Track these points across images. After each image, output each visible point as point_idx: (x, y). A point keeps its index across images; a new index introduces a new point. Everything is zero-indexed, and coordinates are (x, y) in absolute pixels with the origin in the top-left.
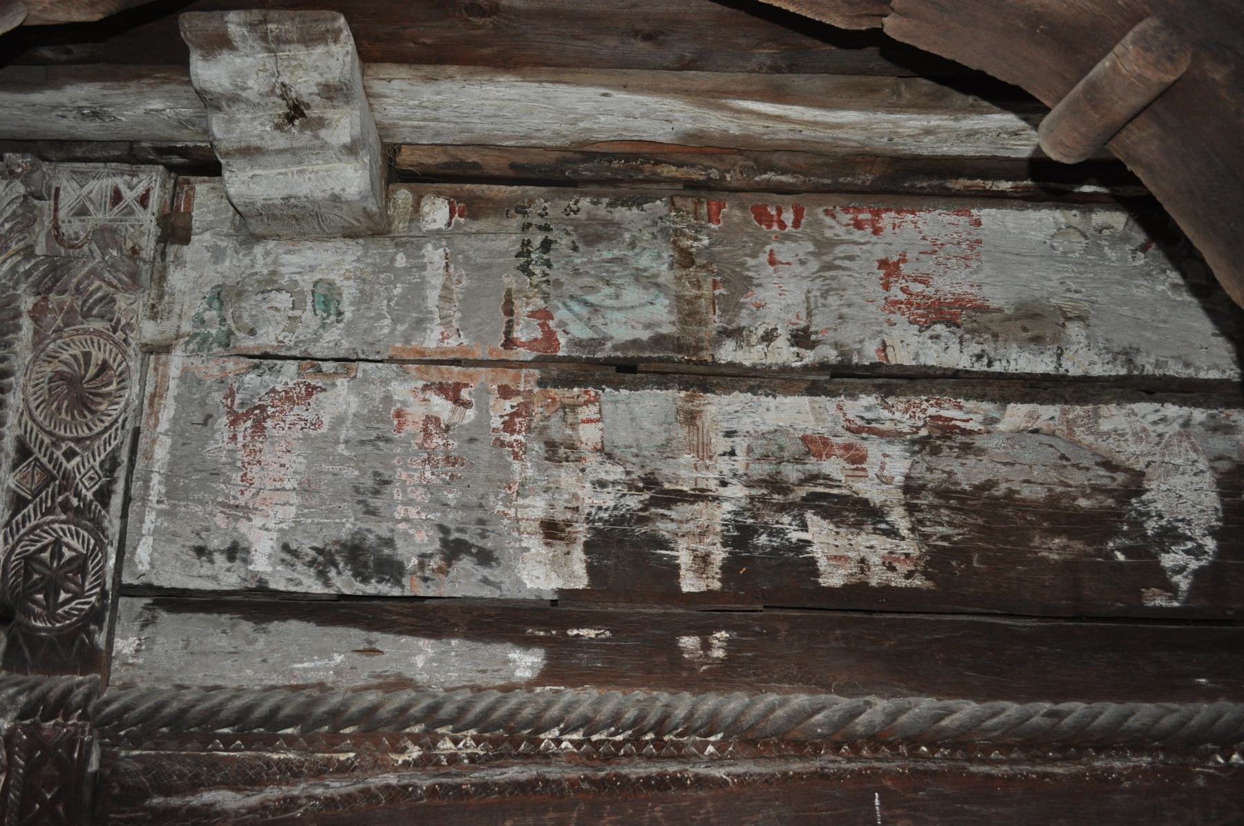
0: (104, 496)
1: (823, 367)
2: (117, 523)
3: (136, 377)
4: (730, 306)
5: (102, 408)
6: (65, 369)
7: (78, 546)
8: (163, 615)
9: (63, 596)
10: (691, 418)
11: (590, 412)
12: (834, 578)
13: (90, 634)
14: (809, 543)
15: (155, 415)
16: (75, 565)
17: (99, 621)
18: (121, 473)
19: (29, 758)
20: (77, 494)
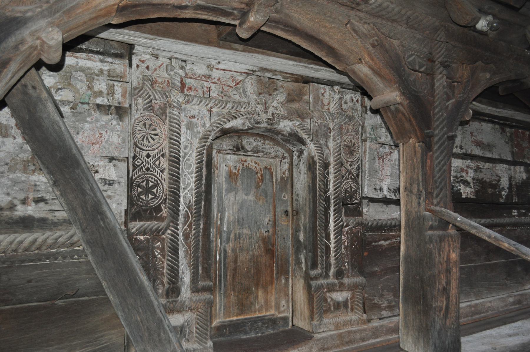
0: (358, 175)
1: (463, 154)
8: (371, 203)
9: (353, 199)
12: (464, 196)
14: (460, 189)
15: (365, 156)
18: (360, 170)
19: (351, 236)
20: (353, 175)
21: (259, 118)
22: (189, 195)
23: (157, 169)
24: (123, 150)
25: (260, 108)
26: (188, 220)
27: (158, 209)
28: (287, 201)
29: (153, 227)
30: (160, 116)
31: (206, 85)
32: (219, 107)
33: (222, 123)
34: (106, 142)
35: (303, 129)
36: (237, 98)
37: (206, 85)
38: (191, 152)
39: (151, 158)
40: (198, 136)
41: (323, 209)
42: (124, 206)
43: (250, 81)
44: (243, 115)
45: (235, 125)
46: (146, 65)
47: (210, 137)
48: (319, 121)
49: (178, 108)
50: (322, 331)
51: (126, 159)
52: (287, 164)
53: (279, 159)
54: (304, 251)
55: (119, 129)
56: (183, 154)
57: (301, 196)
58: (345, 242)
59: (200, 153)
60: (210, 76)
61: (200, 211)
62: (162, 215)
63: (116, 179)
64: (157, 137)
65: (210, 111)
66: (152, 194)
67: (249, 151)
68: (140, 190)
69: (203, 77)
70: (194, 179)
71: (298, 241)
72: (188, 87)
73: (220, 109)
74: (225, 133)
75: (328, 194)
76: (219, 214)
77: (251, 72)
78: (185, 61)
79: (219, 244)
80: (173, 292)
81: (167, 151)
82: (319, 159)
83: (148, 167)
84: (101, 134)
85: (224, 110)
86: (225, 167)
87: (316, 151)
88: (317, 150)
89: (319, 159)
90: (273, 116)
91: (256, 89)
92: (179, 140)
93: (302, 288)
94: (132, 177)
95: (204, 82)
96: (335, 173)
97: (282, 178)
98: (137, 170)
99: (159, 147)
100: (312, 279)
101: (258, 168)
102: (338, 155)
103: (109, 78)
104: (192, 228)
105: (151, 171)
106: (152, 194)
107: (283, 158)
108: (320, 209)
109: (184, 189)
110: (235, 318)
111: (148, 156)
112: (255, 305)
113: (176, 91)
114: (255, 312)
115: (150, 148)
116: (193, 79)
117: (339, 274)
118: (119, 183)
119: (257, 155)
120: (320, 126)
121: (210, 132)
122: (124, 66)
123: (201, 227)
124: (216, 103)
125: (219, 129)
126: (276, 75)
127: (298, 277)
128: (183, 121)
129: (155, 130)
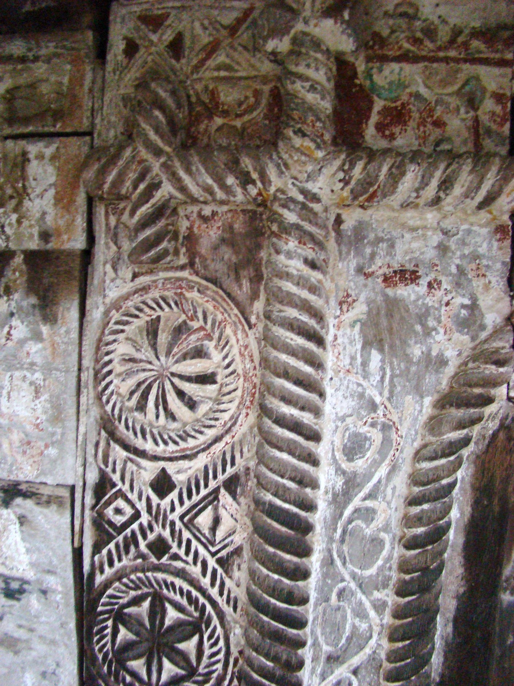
24: (52, 451)
30: (229, 283)
31: (492, 86)
37: (492, 86)
38: (382, 471)
39: (174, 495)
40: (429, 379)
46: (169, 36)
49: (305, 237)
51: (66, 494)
55: (38, 360)
56: (340, 483)
63: (30, 575)
64: (211, 389)
66: (179, 658)
68: (124, 634)
72: (385, 111)
83: (160, 539)
94: (92, 576)
95: (482, 70)
98: (112, 546)
99: (217, 439)
103: (7, 131)
105: (176, 557)
106: (179, 658)
109: (333, 660)
111: (163, 485)
113: (297, 141)
115: (172, 447)
116: (415, 59)
118: (44, 592)
121: (499, 363)
122: (76, 61)
128: (345, 302)
129: (199, 353)
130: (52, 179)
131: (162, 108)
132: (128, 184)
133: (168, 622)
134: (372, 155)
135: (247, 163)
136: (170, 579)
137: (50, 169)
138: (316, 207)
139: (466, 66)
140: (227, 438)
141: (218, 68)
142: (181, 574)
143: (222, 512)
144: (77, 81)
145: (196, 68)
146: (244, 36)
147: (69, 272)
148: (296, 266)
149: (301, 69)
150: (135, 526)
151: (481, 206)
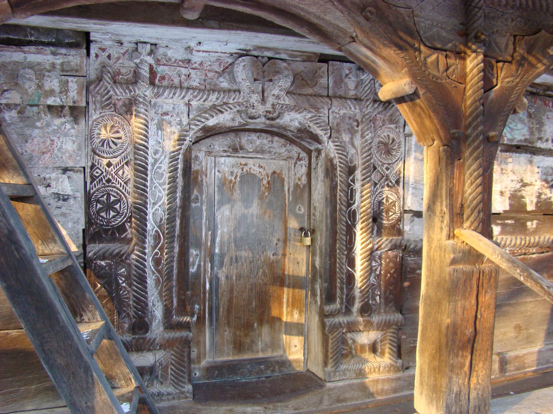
0: (398, 182)
2: (402, 190)
3: (403, 144)
4: (540, 130)
5: (394, 153)
6: (382, 140)
7: (393, 198)
9: (391, 214)
10: (531, 162)
11: (510, 160)
13: (399, 225)
14: (551, 197)
16: (392, 204)
17: (400, 221)
19: (385, 262)
20: (391, 182)
21: (254, 111)
22: (160, 212)
23: (120, 181)
24: (78, 158)
25: (255, 98)
26: (159, 243)
27: (122, 229)
28: (303, 215)
29: (114, 251)
31: (184, 73)
32: (199, 100)
33: (203, 120)
34: (59, 150)
35: (317, 123)
36: (225, 85)
37: (184, 73)
38: (163, 157)
39: (112, 167)
40: (172, 137)
41: (344, 228)
42: (82, 226)
43: (242, 64)
44: (231, 109)
45: (221, 122)
46: (107, 54)
47: (188, 138)
48: (342, 112)
50: (338, 379)
51: (82, 169)
52: (304, 167)
53: (294, 161)
54: (319, 281)
55: (74, 134)
56: (153, 161)
57: (318, 209)
58: (376, 270)
59: (174, 159)
60: (189, 61)
61: (174, 231)
62: (126, 236)
65: (188, 105)
66: (115, 210)
67: (250, 152)
68: (99, 206)
69: (180, 63)
70: (167, 192)
71: (314, 266)
72: (160, 77)
73: (201, 102)
74: (209, 133)
75: (354, 207)
76: (210, 233)
77: (244, 52)
78: (156, 45)
79: (209, 270)
80: (140, 329)
81: (133, 158)
82: (340, 162)
83: (109, 179)
84: (52, 141)
85: (206, 103)
86: (217, 173)
87: (335, 151)
88: (338, 150)
89: (340, 162)
90: (273, 108)
91: (250, 75)
92: (146, 144)
93: (316, 327)
94: (90, 191)
95: (182, 69)
96: (363, 180)
97: (297, 186)
98: (95, 182)
99: (123, 153)
100: (327, 316)
101: (264, 173)
102: (367, 156)
103: (62, 74)
104: (164, 252)
105: (113, 183)
106: (115, 210)
107: (299, 159)
108: (341, 227)
109: (154, 204)
110: (231, 358)
112: (257, 345)
113: (142, 83)
114: (258, 352)
115: (111, 155)
116: (167, 65)
117: (366, 310)
118: (75, 198)
119: (262, 156)
120: (343, 118)
121: (187, 132)
122: (81, 57)
123: (177, 250)
124: (195, 94)
125: (200, 127)
126: (279, 53)
127: (313, 312)
128: (152, 120)
129: (117, 132)
130: (76, 88)
131: (110, 73)
132: (102, 90)
133: (111, 201)
134: (158, 87)
135: (131, 87)
136: (112, 189)
137: (75, 85)
138: (147, 98)
139: (178, 68)
140: (125, 152)
141: (120, 64)
142: (114, 187)
143: (125, 170)
144: (82, 62)
145: (115, 63)
146: (127, 56)
147: (82, 112)
148: (143, 111)
149: (142, 67)
150: (102, 176)
151: (182, 99)
